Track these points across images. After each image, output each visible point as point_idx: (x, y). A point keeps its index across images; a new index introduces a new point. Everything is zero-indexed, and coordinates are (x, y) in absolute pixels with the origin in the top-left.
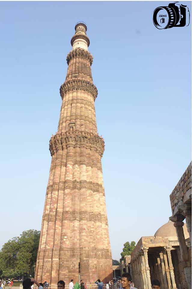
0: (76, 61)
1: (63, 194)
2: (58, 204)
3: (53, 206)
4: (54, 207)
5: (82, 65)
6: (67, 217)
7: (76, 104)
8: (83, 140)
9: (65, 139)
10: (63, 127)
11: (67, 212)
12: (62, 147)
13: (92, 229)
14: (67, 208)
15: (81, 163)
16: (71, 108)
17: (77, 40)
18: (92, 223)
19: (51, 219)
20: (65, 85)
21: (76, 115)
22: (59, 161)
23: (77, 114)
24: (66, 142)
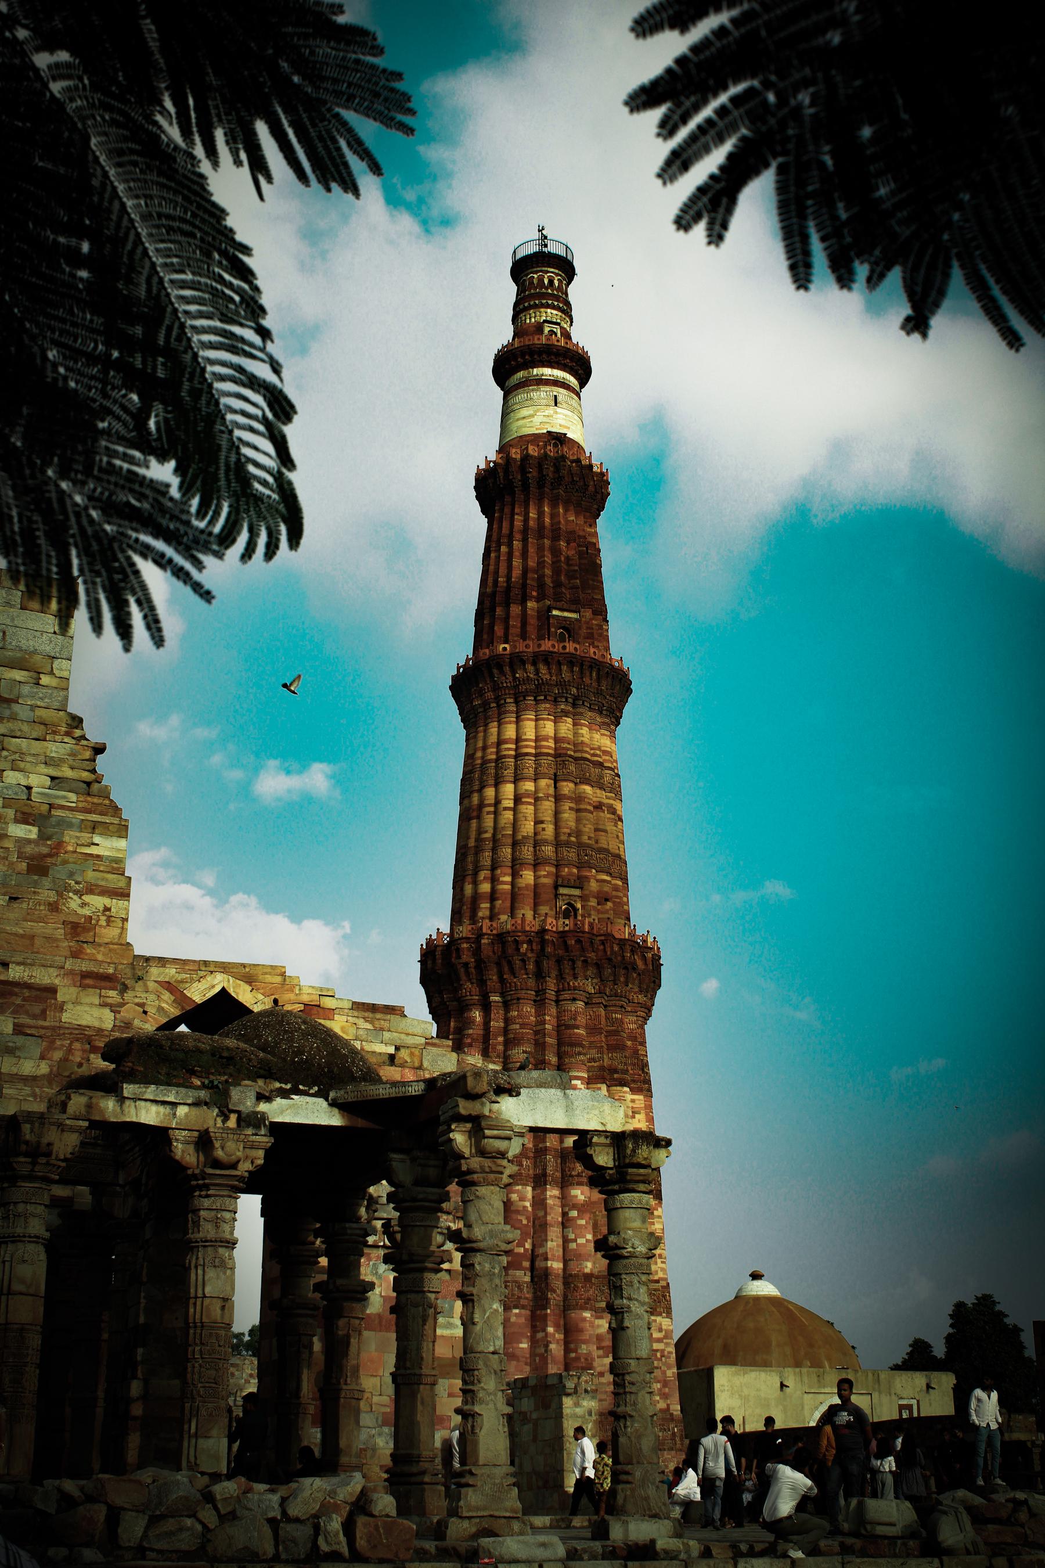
0: (553, 516)
1: (558, 1202)
2: (550, 1244)
3: (524, 1246)
4: (526, 1250)
5: (581, 555)
6: (589, 1299)
7: (576, 784)
8: (622, 979)
9: (559, 961)
10: (527, 885)
11: (588, 1277)
12: (540, 992)
13: (655, 1346)
14: (587, 1260)
15: (616, 1076)
16: (558, 798)
17: (547, 372)
18: (655, 1321)
19: (519, 1298)
20: (523, 662)
21: (580, 845)
22: (524, 1052)
23: (585, 839)
24: (560, 977)
